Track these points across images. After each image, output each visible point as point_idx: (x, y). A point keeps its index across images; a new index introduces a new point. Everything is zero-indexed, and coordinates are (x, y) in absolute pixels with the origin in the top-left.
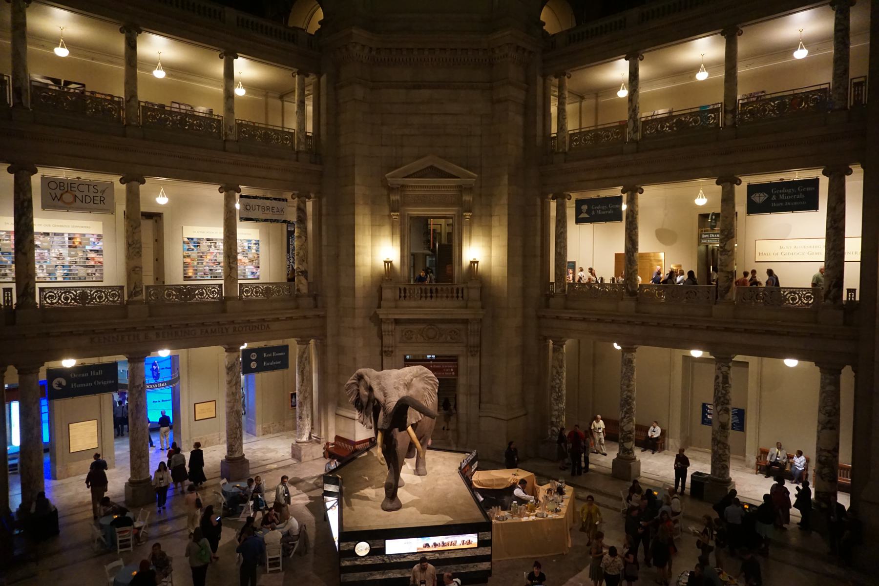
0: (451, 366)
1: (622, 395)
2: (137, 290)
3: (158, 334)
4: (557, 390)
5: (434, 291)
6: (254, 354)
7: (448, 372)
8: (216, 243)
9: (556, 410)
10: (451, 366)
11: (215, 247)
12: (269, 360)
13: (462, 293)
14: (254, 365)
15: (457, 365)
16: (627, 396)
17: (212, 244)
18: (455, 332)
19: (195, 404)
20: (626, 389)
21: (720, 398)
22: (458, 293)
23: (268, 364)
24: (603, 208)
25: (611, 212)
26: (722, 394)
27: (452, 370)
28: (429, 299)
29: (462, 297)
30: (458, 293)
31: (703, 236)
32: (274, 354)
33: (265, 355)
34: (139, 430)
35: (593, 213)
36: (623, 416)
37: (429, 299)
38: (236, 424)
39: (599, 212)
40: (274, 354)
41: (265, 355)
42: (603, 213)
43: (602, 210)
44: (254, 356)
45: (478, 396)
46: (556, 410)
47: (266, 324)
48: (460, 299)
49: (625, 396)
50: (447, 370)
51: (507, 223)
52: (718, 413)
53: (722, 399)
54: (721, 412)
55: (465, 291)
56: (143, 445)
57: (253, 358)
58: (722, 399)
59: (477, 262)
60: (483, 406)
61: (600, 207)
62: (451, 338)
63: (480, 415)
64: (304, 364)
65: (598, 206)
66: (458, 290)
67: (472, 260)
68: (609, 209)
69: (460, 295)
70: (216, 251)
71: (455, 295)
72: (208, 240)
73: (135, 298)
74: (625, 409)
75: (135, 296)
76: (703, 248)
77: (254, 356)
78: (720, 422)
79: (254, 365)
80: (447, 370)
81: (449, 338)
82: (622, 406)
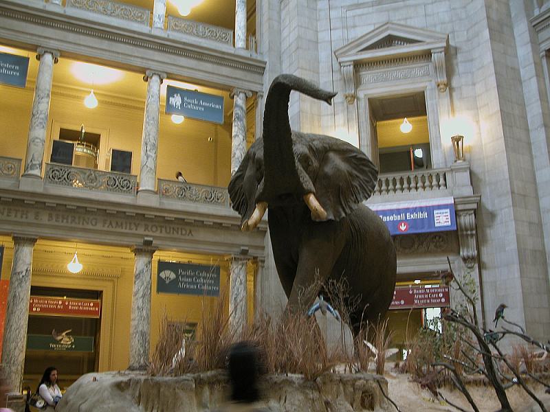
0: (439, 290)
2: (34, 162)
7: (436, 298)
10: (439, 290)
13: (445, 180)
18: (440, 238)
22: (438, 181)
27: (441, 295)
34: (13, 328)
38: (139, 350)
47: (188, 228)
48: (442, 187)
56: (15, 349)
66: (438, 175)
71: (434, 182)
73: (31, 172)
75: (31, 169)
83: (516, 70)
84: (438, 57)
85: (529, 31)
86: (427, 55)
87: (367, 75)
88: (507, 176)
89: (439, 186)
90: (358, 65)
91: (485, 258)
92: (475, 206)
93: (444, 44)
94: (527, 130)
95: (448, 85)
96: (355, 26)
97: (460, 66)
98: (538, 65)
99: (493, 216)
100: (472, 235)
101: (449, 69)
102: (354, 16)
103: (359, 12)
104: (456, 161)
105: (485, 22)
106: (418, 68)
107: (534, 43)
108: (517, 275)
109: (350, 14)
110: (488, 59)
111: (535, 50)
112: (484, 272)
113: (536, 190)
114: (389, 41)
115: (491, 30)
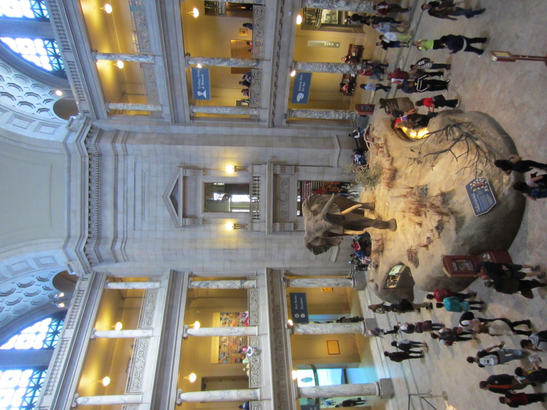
1: (326, 72)
3: (282, 379)
4: (322, 115)
5: (254, 193)
6: (295, 316)
8: (222, 342)
9: (335, 116)
11: (225, 342)
12: (299, 305)
13: (256, 177)
14: (303, 316)
15: (304, 181)
16: (327, 68)
17: (223, 344)
19: (329, 354)
20: (321, 69)
21: (329, 5)
22: (256, 180)
23: (302, 306)
24: (199, 81)
25: (202, 76)
26: (326, 4)
27: (307, 185)
28: (260, 189)
29: (259, 177)
30: (256, 180)
31: (220, 12)
32: (296, 302)
33: (296, 308)
35: (203, 88)
36: (339, 71)
37: (260, 189)
39: (203, 84)
40: (296, 302)
41: (296, 308)
42: (203, 80)
43: (201, 82)
44: (297, 316)
45: (325, 168)
46: (335, 116)
48: (260, 179)
49: (326, 69)
50: (307, 188)
51: (210, 147)
52: (338, 7)
53: (330, 4)
54: (338, 5)
55: (254, 175)
57: (298, 316)
58: (330, 4)
59: (235, 167)
60: (330, 165)
61: (199, 83)
62: (286, 185)
63: (336, 165)
64: (303, 283)
65: (198, 84)
67: (233, 171)
68: (201, 77)
69: (257, 179)
70: (228, 341)
71: (257, 182)
72: (220, 347)
74: (335, 70)
76: (228, 13)
77: (297, 316)
78: (345, 6)
79: (303, 316)
80: (307, 188)
81: (286, 187)
82: (333, 72)
83: (199, 136)
84: (188, 173)
85: (178, 126)
86: (185, 178)
87: (190, 212)
88: (258, 148)
89: (259, 180)
90: (184, 216)
91: (293, 163)
92: (272, 165)
93: (182, 169)
94: (232, 135)
95: (204, 170)
96: (156, 217)
97: (193, 163)
98: (198, 125)
99: (274, 157)
100: (284, 168)
101: (195, 168)
102: (149, 216)
103: (146, 214)
104: (248, 171)
105: (172, 147)
106: (190, 184)
107: (185, 124)
108: (304, 150)
109: (147, 219)
110: (193, 148)
111: (190, 125)
112: (300, 164)
113: (262, 136)
114: (173, 198)
115: (177, 144)
